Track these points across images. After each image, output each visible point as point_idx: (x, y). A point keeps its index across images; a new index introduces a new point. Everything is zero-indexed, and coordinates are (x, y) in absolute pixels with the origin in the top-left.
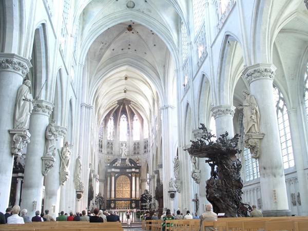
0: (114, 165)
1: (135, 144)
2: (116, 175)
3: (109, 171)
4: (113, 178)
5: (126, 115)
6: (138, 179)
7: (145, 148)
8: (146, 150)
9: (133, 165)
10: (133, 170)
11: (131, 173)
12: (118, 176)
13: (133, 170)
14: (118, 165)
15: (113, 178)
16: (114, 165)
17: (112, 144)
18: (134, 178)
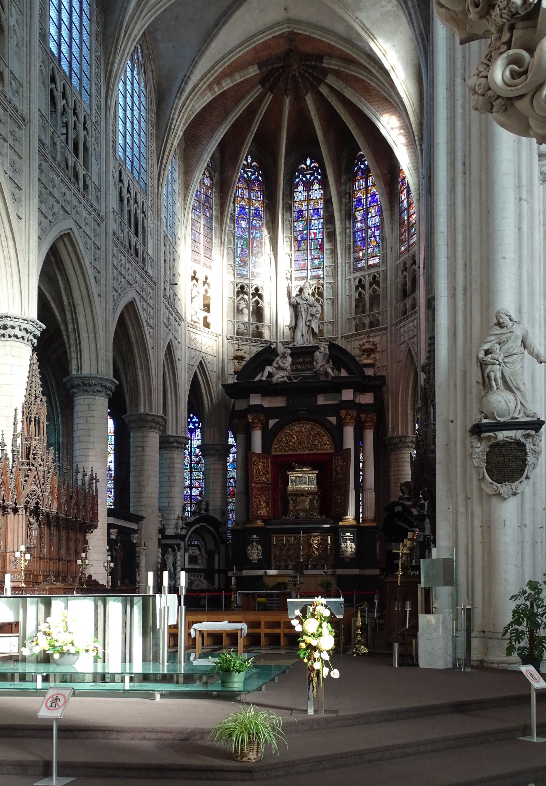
0: (257, 379)
1: (361, 285)
2: (272, 422)
3: (241, 405)
4: (257, 436)
5: (317, 157)
6: (369, 436)
7: (405, 294)
8: (409, 302)
9: (344, 373)
10: (347, 395)
11: (335, 410)
12: (278, 428)
13: (347, 395)
14: (279, 377)
15: (257, 436)
16: (257, 379)
17: (257, 293)
18: (349, 432)
